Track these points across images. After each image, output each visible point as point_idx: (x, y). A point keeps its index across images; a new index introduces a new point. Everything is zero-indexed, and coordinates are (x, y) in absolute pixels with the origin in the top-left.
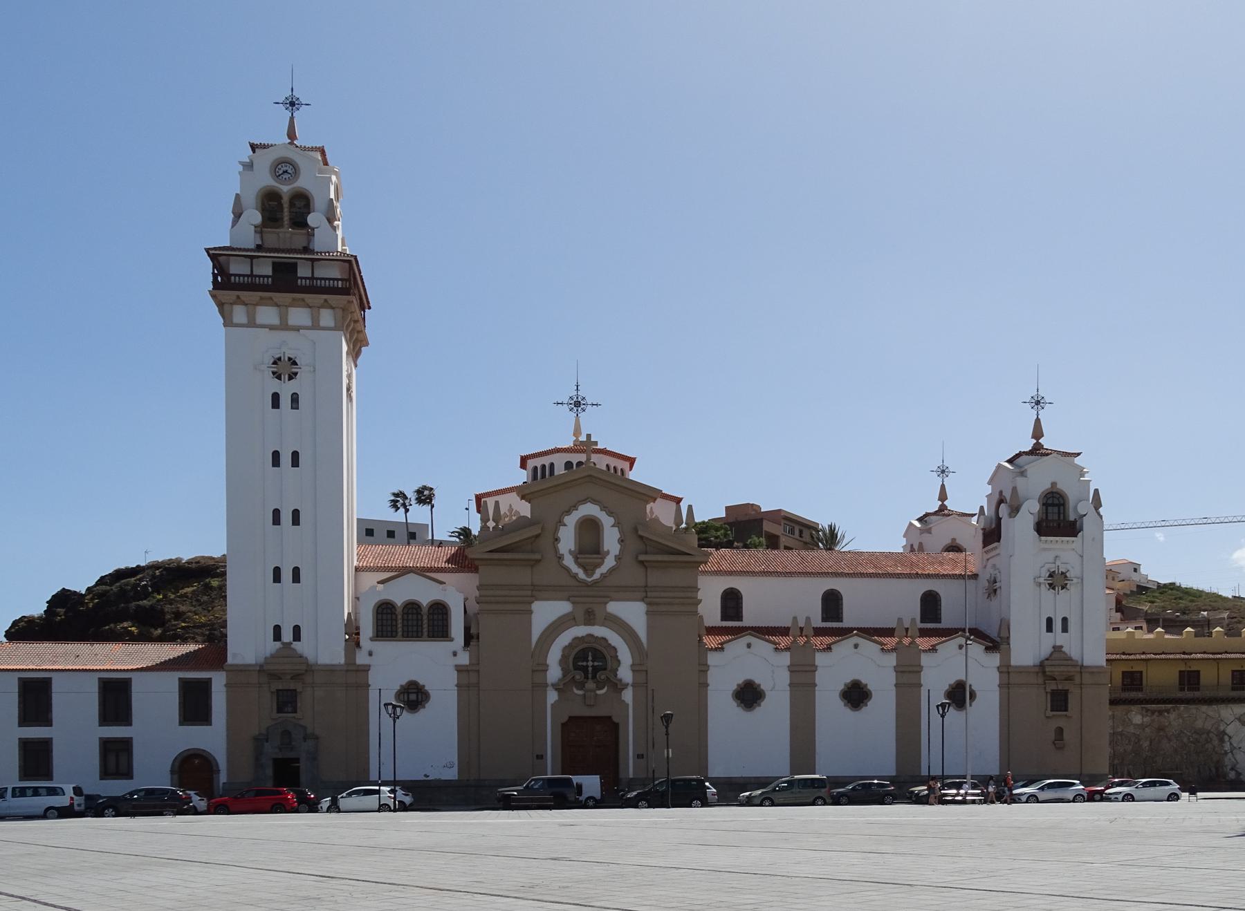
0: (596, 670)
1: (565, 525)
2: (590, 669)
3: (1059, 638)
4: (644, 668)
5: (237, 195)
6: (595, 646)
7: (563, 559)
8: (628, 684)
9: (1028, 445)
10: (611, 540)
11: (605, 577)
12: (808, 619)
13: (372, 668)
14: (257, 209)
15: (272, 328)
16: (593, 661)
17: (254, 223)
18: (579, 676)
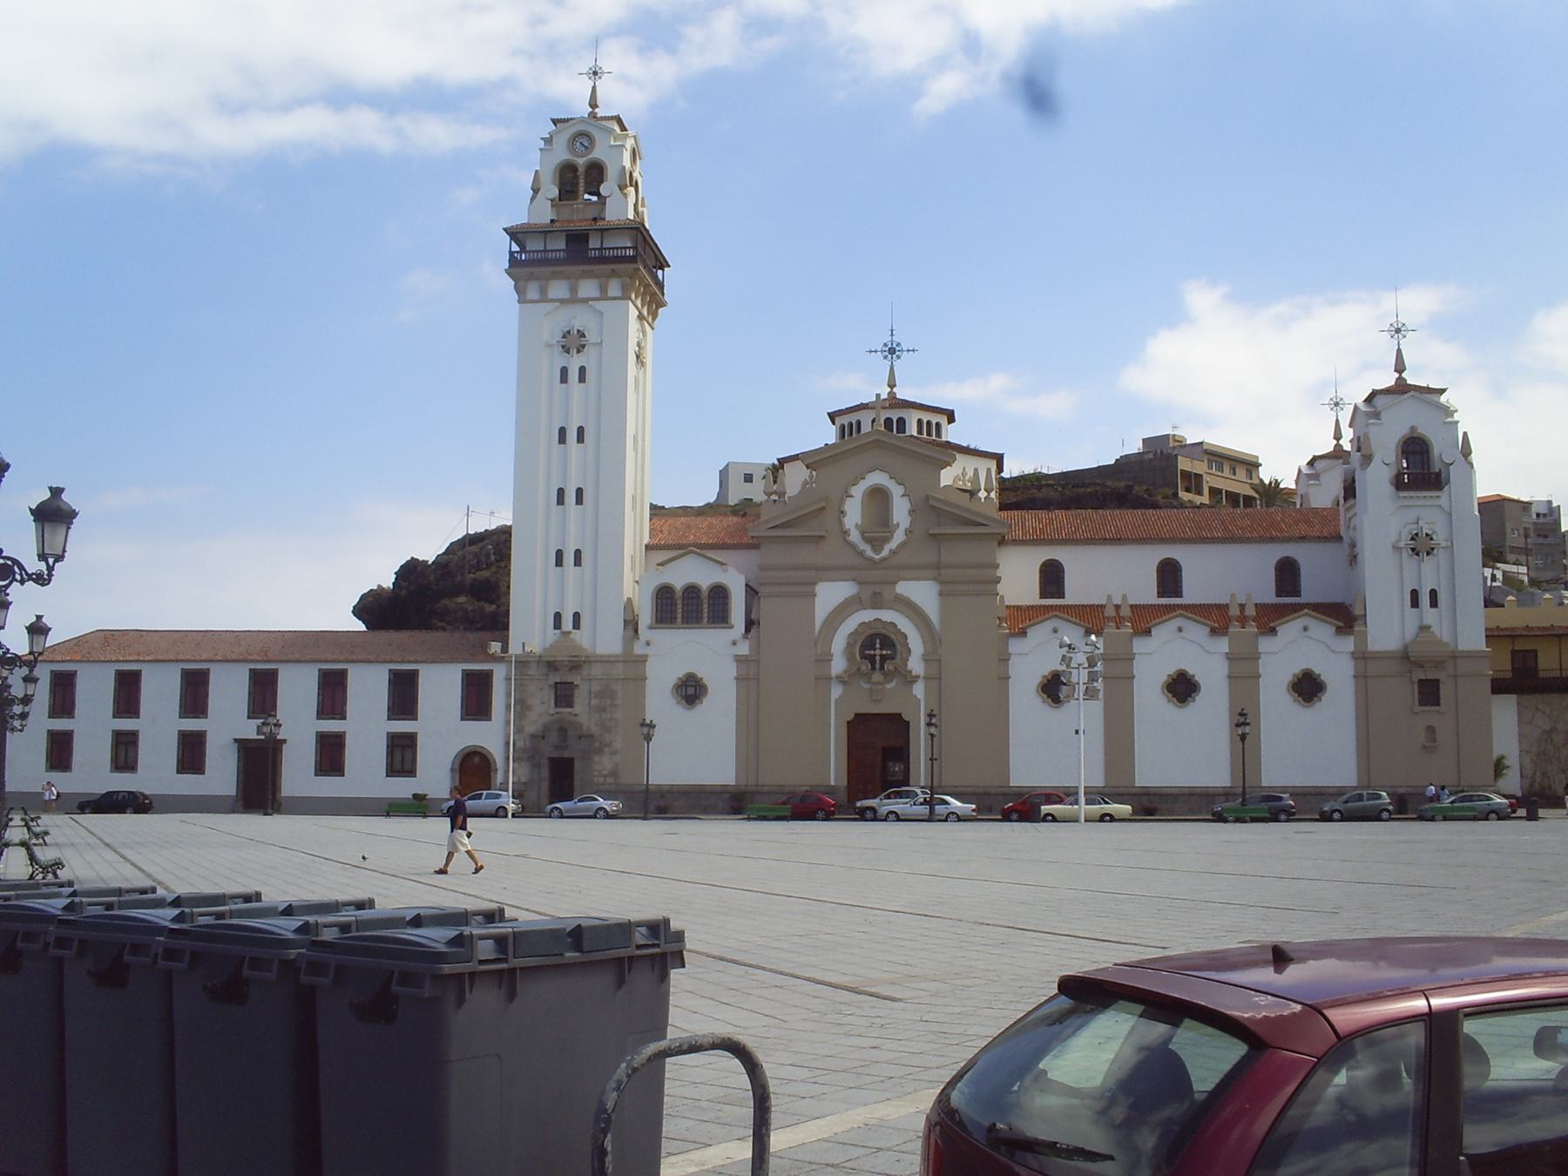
0: (884, 658)
1: (852, 496)
2: (878, 658)
3: (1429, 615)
4: (937, 657)
5: (537, 171)
6: (884, 631)
7: (849, 535)
8: (918, 677)
9: (1389, 380)
10: (901, 512)
11: (894, 553)
12: (1124, 596)
13: (650, 659)
14: (555, 185)
15: (562, 301)
16: (881, 649)
17: (549, 197)
18: (865, 667)
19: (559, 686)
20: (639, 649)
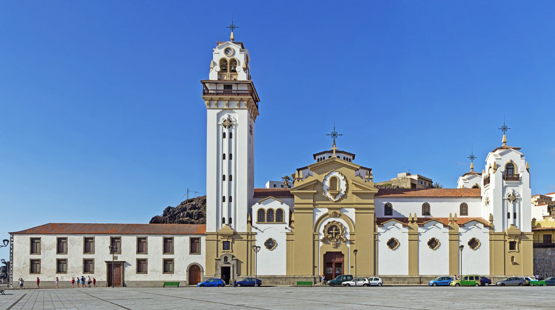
0: (336, 234)
16: (335, 231)
19: (224, 243)
20: (254, 230)
